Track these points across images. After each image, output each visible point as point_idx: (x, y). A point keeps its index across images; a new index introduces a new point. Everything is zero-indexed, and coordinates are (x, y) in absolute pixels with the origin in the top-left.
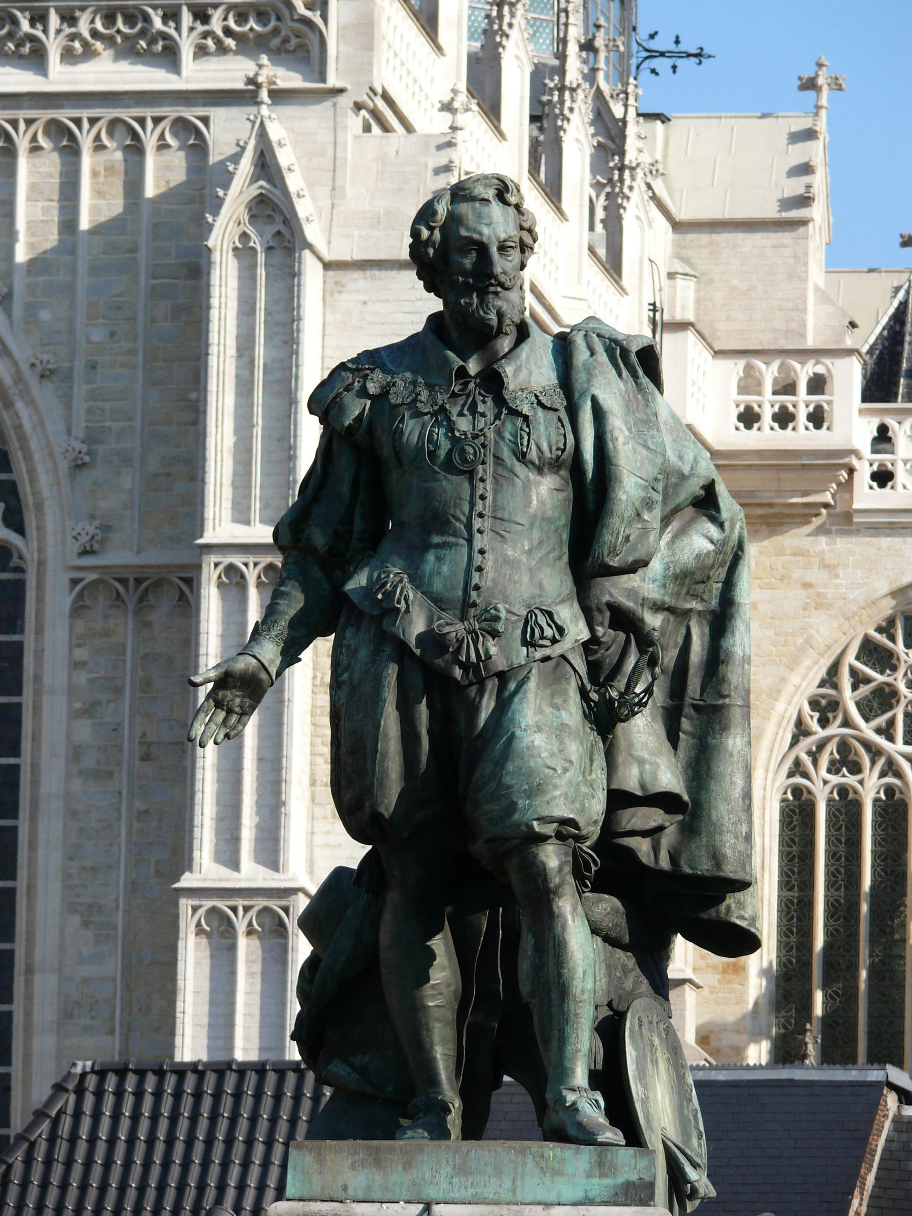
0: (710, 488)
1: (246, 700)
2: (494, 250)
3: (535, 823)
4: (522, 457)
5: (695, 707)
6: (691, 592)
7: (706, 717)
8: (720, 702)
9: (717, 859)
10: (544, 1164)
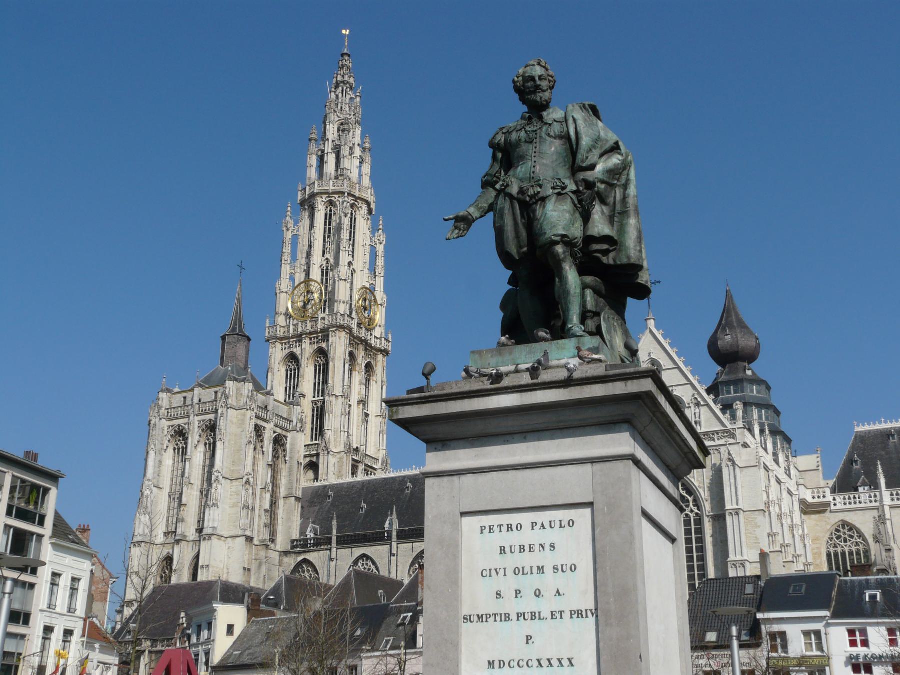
0: (617, 143)
2: (537, 79)
4: (549, 135)
9: (629, 258)
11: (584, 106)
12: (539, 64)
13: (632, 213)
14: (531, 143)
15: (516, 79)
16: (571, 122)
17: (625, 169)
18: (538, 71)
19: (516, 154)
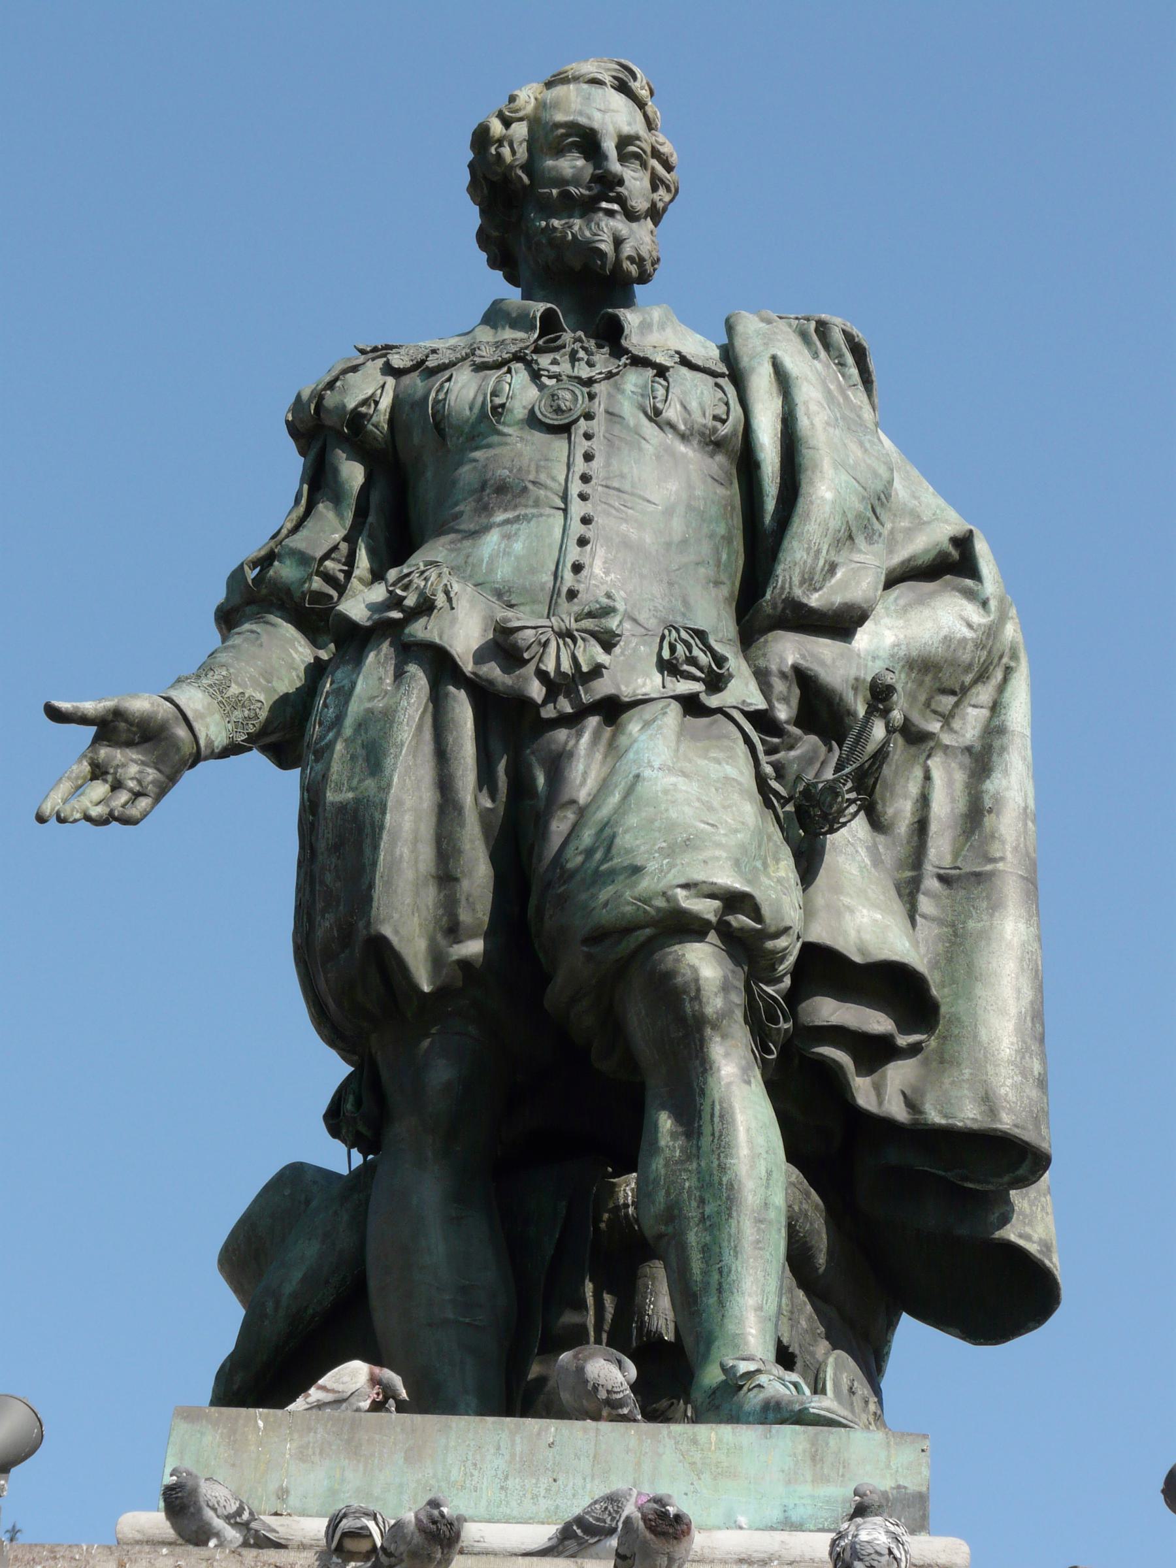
0: (963, 543)
1: (150, 770)
2: (609, 146)
3: (681, 893)
4: (655, 416)
5: (942, 878)
6: (933, 706)
7: (962, 893)
8: (989, 867)
9: (988, 1101)
10: (697, 1457)
11: (822, 328)
12: (622, 87)
13: (1012, 890)
14: (564, 429)
15: (497, 128)
16: (762, 383)
17: (982, 676)
18: (613, 116)
19: (466, 474)
